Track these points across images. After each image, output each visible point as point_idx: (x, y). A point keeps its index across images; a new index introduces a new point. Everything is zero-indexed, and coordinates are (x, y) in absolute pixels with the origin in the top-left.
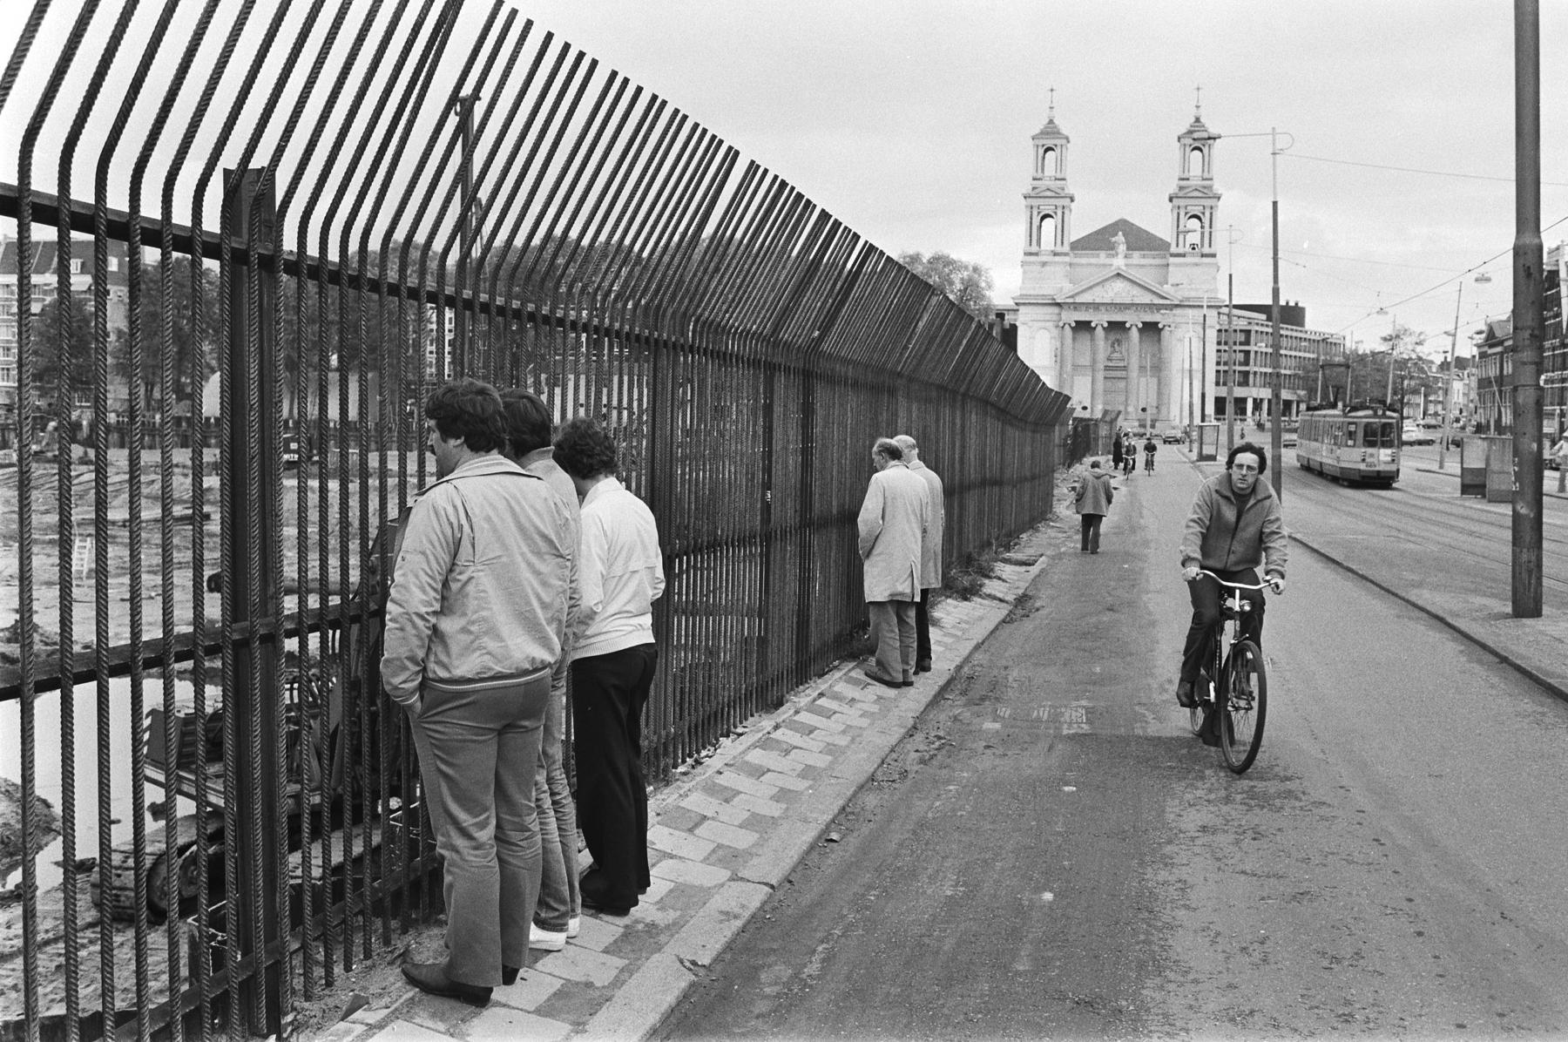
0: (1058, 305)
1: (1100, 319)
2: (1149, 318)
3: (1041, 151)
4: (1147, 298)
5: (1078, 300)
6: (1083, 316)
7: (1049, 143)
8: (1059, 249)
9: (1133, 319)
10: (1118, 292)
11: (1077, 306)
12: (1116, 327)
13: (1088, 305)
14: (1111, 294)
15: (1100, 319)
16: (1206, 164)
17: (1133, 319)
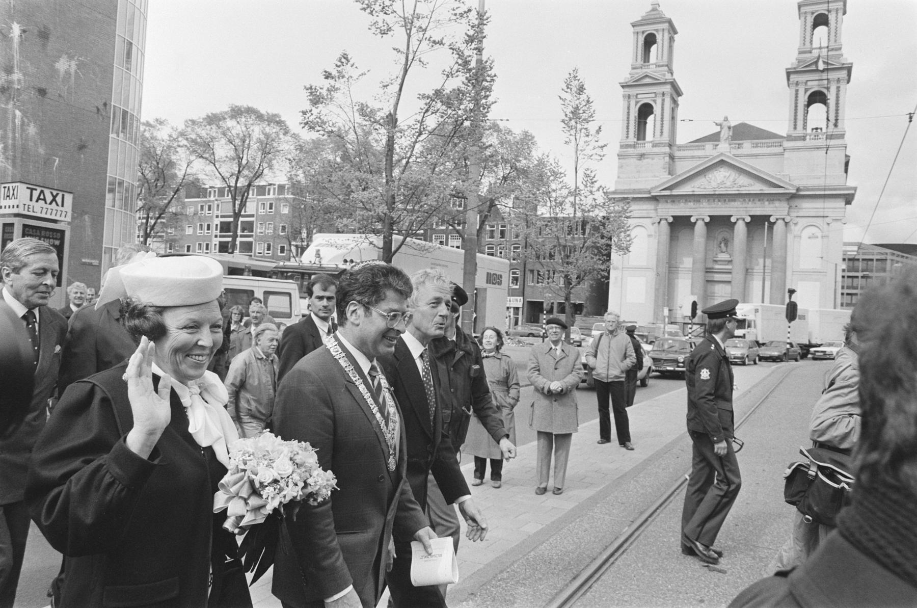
0: (655, 199)
1: (701, 213)
3: (641, 39)
4: (757, 188)
5: (675, 192)
6: (681, 210)
7: (650, 29)
8: (658, 139)
9: (740, 212)
10: (720, 180)
11: (674, 199)
12: (719, 223)
13: (687, 198)
14: (714, 184)
15: (701, 213)
16: (835, 35)
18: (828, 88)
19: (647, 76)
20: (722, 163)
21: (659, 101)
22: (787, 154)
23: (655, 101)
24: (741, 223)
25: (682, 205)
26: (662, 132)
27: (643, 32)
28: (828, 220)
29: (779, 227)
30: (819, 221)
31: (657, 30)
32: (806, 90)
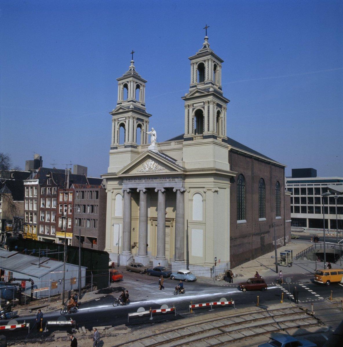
1: (141, 186)
2: (168, 185)
17: (159, 186)
18: (204, 108)
19: (121, 108)
20: (148, 157)
21: (127, 121)
22: (184, 149)
23: (125, 122)
24: (160, 192)
25: (133, 181)
26: (128, 139)
27: (122, 83)
28: (205, 190)
29: (179, 195)
30: (201, 190)
31: (128, 82)
32: (193, 109)
